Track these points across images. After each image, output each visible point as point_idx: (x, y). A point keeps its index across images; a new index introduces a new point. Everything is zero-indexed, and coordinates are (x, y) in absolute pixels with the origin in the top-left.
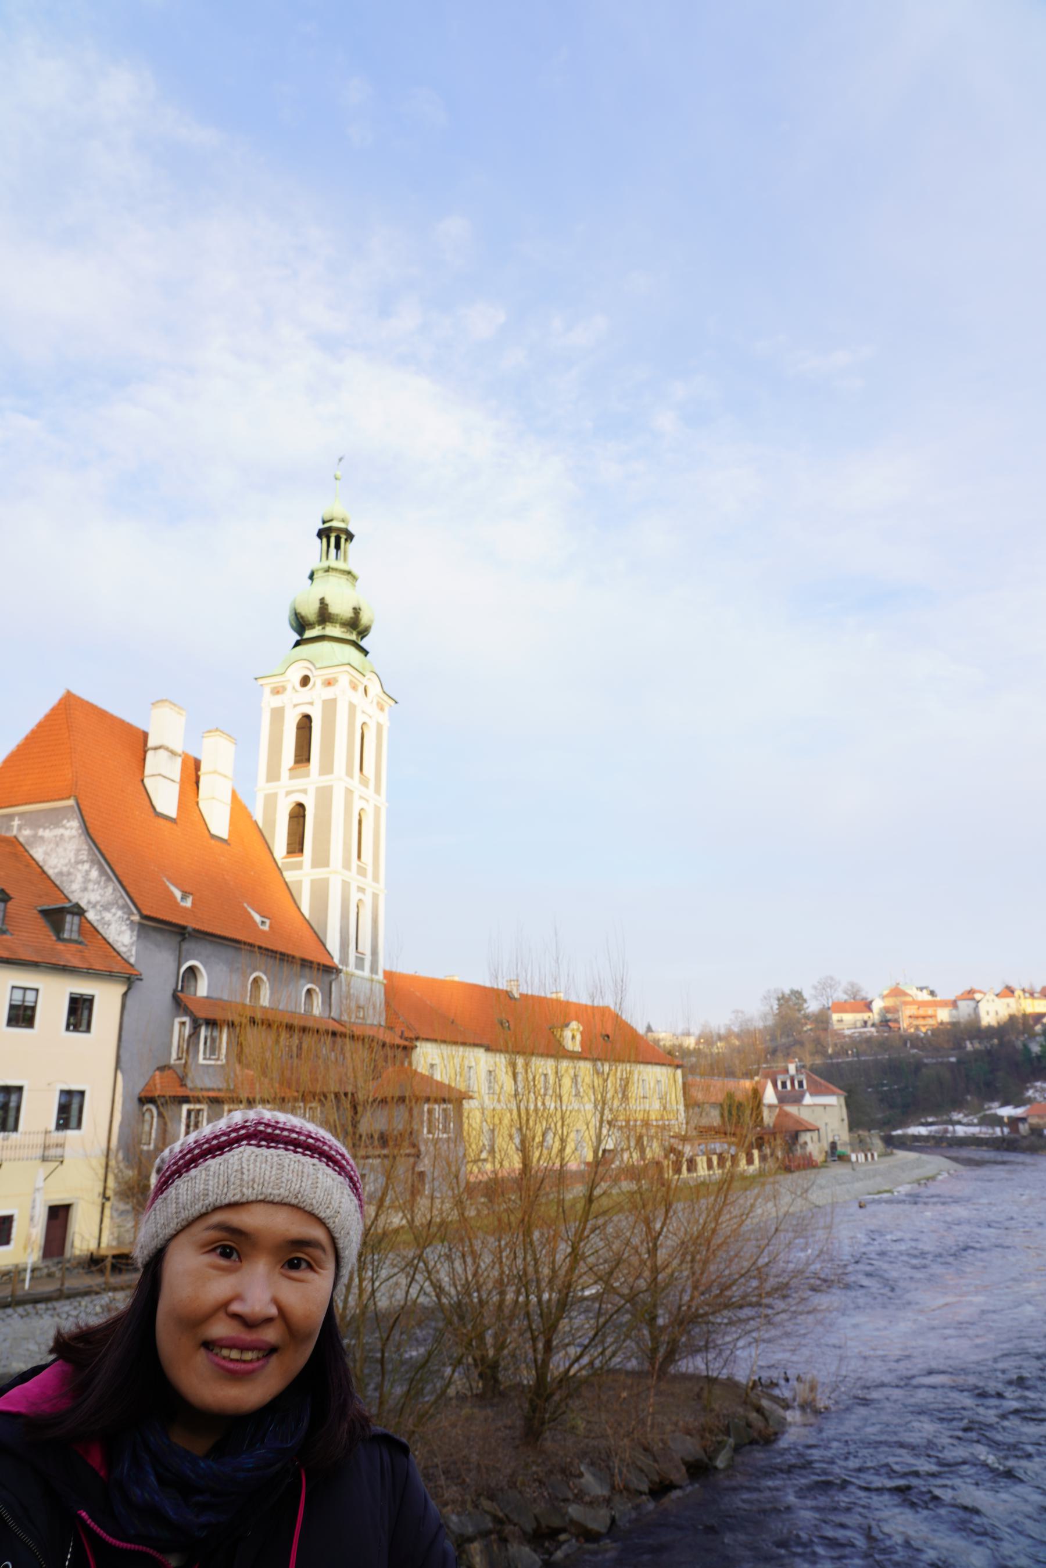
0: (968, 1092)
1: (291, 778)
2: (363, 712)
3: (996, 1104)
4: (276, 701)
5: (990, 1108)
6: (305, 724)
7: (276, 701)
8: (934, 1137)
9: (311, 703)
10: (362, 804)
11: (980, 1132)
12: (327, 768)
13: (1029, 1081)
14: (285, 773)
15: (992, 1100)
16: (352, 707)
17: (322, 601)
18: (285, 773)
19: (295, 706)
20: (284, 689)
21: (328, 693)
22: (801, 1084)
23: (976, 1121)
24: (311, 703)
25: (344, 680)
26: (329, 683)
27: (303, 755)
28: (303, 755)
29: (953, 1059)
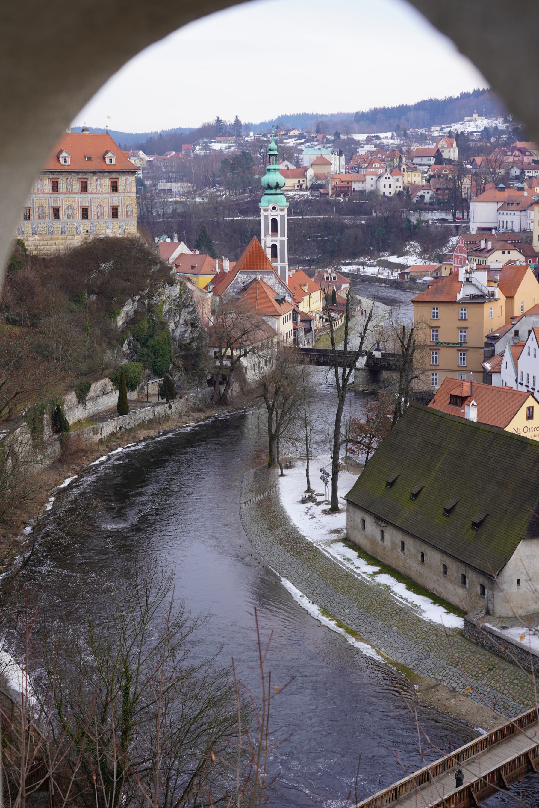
0: (371, 245)
3: (387, 254)
4: (266, 213)
5: (383, 256)
6: (274, 221)
7: (266, 213)
8: (352, 274)
11: (379, 273)
13: (407, 241)
15: (385, 251)
17: (277, 183)
21: (282, 213)
22: (334, 278)
23: (375, 263)
26: (282, 210)
29: (363, 222)
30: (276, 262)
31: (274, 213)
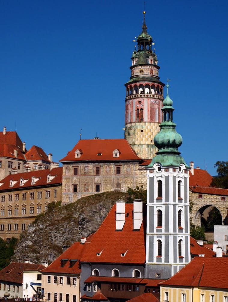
1: (157, 202)
2: (179, 177)
4: (151, 175)
7: (151, 175)
9: (162, 177)
10: (180, 208)
12: (167, 199)
14: (155, 201)
16: (174, 177)
18: (155, 201)
19: (157, 177)
20: (154, 171)
21: (166, 174)
24: (162, 177)
25: (171, 170)
26: (167, 170)
27: (160, 194)
28: (160, 194)
30: (161, 232)
31: (159, 174)
